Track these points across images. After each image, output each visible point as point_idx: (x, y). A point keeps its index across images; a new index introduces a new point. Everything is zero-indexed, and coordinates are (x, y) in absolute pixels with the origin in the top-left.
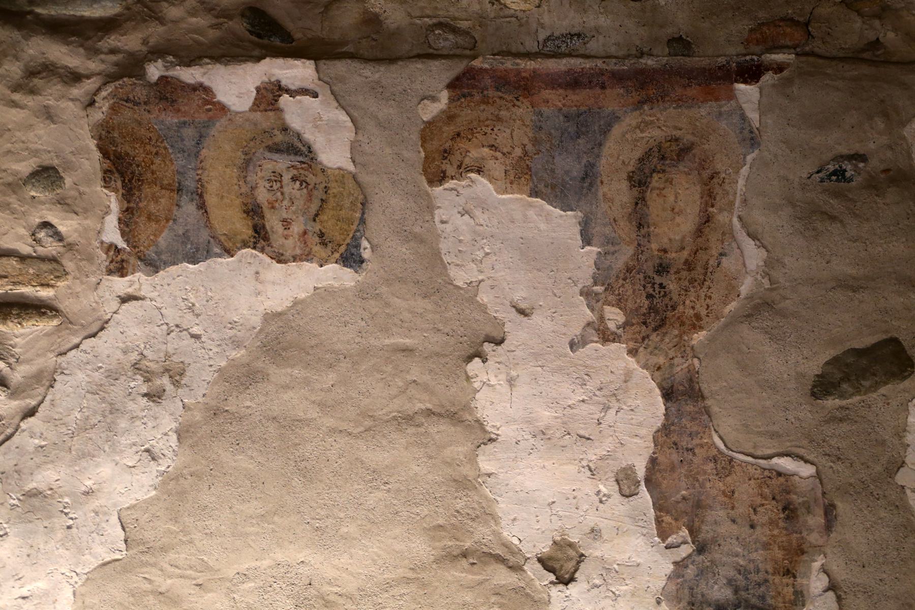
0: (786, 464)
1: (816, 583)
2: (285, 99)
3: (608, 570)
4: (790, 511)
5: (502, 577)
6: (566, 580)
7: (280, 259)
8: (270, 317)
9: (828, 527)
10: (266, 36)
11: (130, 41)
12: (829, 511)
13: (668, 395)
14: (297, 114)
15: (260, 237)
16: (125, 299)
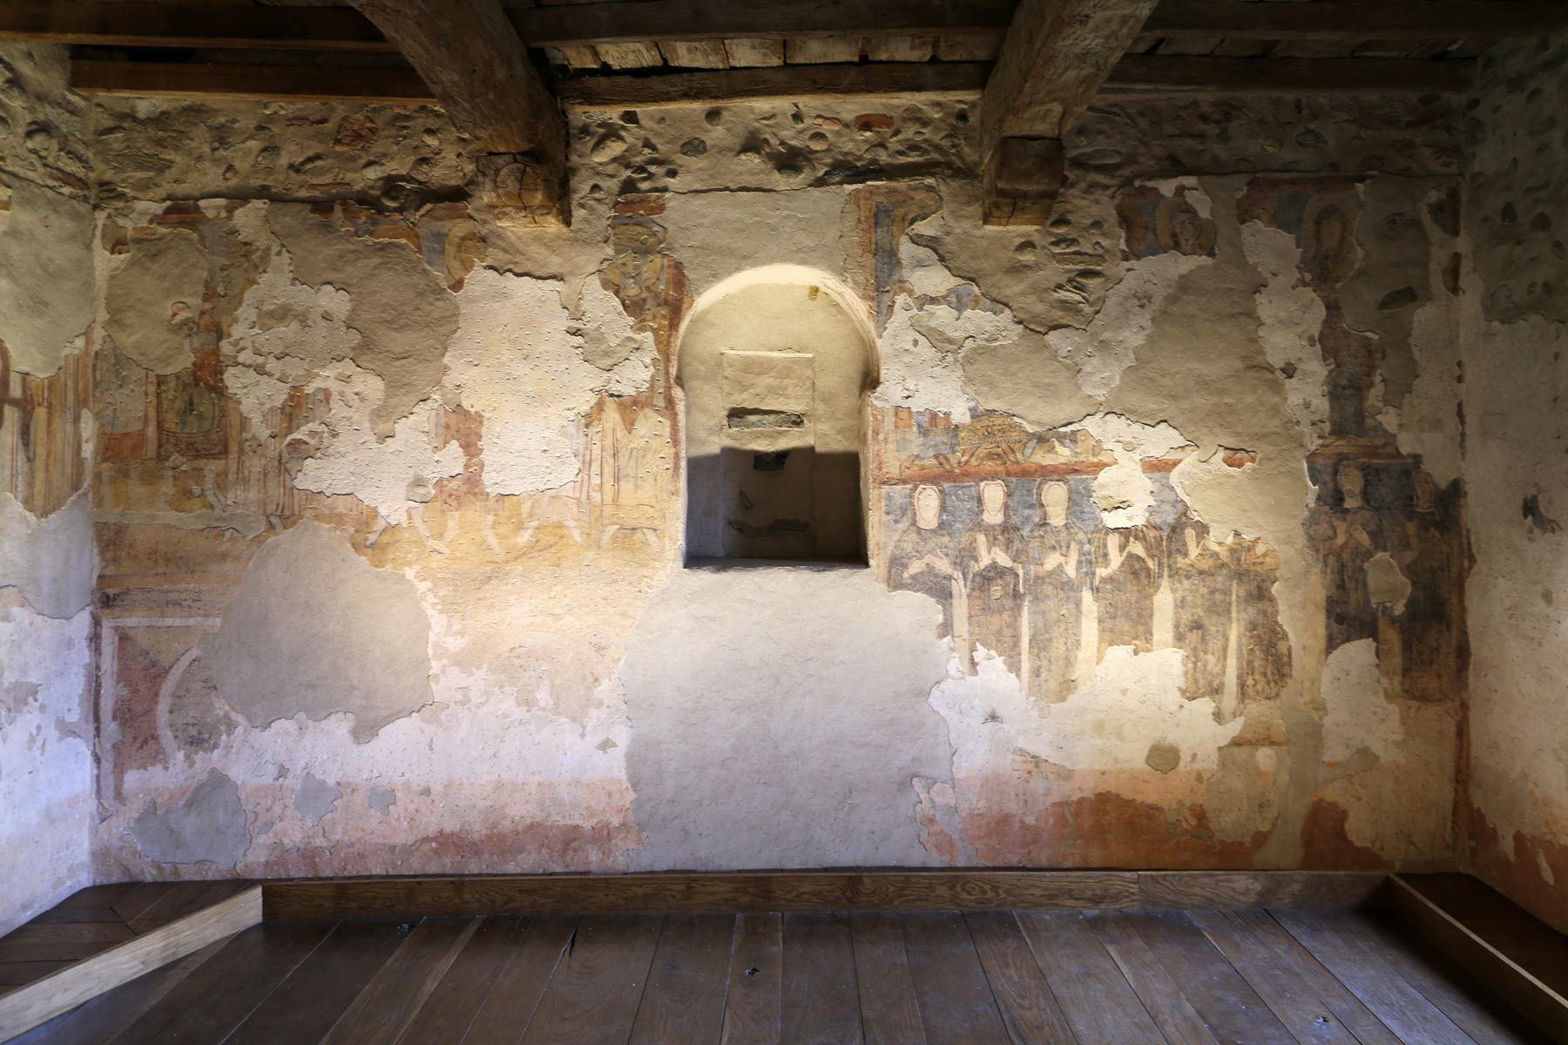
0: (1369, 334)
1: (1378, 379)
3: (1305, 373)
4: (1370, 353)
5: (1268, 375)
6: (1290, 377)
12: (1384, 352)
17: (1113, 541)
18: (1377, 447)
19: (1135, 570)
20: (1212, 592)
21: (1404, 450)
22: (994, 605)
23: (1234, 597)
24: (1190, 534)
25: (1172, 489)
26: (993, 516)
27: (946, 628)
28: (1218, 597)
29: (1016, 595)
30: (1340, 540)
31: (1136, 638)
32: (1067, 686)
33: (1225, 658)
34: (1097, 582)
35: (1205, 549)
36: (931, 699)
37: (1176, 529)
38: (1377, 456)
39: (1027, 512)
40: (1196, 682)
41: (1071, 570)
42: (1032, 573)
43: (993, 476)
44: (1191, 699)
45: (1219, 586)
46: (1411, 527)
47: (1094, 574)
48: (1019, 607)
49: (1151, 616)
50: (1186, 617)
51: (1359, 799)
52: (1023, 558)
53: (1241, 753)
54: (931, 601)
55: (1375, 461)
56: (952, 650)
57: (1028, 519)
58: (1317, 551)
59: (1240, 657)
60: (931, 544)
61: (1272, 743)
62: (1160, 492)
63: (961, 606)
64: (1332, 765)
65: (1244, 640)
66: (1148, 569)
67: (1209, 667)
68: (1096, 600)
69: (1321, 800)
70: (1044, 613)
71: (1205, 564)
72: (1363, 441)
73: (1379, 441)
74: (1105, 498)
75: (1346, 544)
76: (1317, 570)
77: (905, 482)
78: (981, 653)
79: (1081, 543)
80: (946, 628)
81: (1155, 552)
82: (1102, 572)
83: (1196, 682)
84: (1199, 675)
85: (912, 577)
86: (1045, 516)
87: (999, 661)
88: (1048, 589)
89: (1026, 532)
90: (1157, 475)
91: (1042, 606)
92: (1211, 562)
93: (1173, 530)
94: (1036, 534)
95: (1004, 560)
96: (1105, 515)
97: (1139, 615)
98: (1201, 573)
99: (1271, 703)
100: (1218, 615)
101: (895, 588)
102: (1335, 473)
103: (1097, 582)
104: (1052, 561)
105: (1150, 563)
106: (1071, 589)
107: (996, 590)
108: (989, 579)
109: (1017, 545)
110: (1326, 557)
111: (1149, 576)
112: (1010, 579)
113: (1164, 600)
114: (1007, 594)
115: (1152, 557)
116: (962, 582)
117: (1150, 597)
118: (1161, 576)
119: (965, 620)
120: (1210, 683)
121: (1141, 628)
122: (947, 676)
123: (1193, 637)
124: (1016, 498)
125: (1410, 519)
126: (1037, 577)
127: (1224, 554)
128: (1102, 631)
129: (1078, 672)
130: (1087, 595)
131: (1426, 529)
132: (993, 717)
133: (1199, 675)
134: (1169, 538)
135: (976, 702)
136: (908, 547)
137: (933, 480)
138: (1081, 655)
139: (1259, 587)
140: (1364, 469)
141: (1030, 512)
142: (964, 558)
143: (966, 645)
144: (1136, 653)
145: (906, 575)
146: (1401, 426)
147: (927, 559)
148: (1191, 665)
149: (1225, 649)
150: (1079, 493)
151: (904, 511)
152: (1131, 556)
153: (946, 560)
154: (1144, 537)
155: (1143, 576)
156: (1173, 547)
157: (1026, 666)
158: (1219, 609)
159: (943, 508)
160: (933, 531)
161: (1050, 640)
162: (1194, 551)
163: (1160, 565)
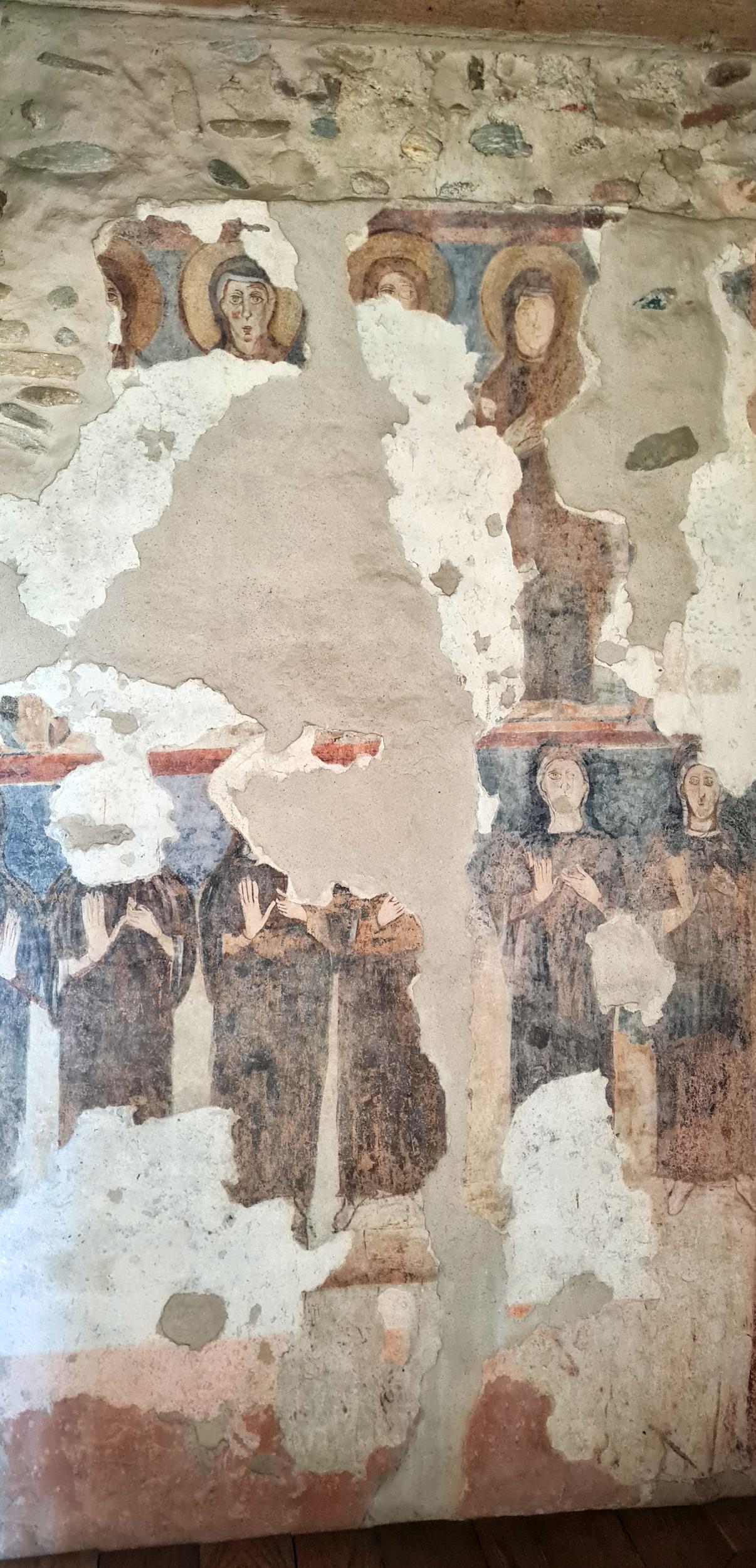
2: (244, 232)
5: (406, 591)
7: (242, 355)
8: (236, 400)
9: (631, 559)
10: (227, 179)
11: (127, 188)
13: (525, 463)
14: (254, 246)
15: (225, 341)
16: (127, 386)
18: (614, 722)
19: (134, 956)
20: (291, 998)
21: (666, 729)
23: (334, 1006)
24: (248, 889)
30: (543, 890)
34: (59, 986)
38: (614, 737)
46: (678, 866)
47: (53, 971)
51: (574, 1371)
53: (346, 1302)
55: (610, 748)
58: (496, 915)
59: (344, 1120)
61: (410, 1277)
64: (521, 1310)
65: (352, 1085)
66: (163, 958)
68: (56, 1021)
69: (503, 1379)
71: (275, 948)
72: (589, 711)
73: (619, 710)
75: (552, 898)
76: (494, 949)
82: (69, 967)
90: (181, 779)
99: (406, 1200)
102: (534, 770)
103: (59, 986)
105: (171, 948)
110: (512, 926)
113: (194, 1015)
115: (173, 934)
117: (164, 1010)
118: (189, 970)
123: (254, 1087)
125: (676, 850)
127: (316, 926)
130: (38, 1015)
131: (708, 869)
134: (207, 899)
139: (383, 985)
140: (588, 762)
144: (138, 1119)
146: (662, 682)
152: (128, 931)
154: (158, 899)
156: (214, 916)
162: (255, 919)
163: (189, 951)
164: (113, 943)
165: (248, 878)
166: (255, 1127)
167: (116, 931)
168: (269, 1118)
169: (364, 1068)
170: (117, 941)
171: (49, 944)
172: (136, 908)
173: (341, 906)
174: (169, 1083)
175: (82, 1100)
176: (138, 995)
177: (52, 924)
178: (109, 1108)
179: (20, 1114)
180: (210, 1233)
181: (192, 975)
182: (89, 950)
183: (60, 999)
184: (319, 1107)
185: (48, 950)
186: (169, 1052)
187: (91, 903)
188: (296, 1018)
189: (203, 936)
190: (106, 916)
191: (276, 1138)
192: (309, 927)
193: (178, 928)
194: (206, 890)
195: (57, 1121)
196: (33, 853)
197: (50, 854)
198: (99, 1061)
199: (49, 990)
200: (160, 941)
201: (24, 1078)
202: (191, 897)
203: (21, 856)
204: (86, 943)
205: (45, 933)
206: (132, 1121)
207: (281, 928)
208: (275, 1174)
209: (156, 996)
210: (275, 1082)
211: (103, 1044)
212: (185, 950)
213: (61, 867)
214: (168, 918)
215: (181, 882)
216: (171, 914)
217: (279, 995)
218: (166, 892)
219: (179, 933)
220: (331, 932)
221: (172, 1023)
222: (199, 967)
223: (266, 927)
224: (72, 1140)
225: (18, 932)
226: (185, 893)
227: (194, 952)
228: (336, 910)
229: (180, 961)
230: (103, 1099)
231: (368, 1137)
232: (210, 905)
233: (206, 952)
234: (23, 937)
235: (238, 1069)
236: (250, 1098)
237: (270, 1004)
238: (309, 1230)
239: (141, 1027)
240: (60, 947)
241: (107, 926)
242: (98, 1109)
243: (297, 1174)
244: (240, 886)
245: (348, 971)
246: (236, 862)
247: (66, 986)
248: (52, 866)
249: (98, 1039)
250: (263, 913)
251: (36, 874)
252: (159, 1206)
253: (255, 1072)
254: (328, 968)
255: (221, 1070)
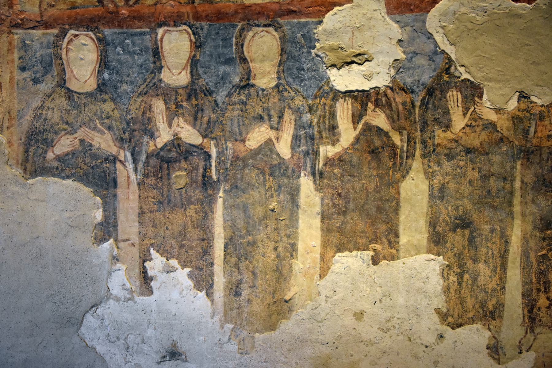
17: (344, 111)
19: (373, 145)
20: (485, 177)
22: (176, 197)
23: (518, 184)
24: (454, 97)
25: (430, 36)
26: (176, 75)
27: (107, 229)
28: (493, 183)
29: (207, 183)
31: (375, 240)
32: (280, 308)
33: (504, 267)
34: (320, 164)
35: (476, 117)
36: (83, 330)
37: (435, 92)
39: (222, 69)
40: (462, 301)
41: (284, 148)
42: (230, 152)
43: (175, 20)
44: (454, 326)
45: (495, 169)
47: (316, 153)
48: (211, 200)
49: (397, 209)
50: (446, 212)
52: (217, 132)
54: (86, 190)
56: (116, 259)
57: (224, 78)
59: (525, 267)
60: (87, 113)
62: (412, 40)
63: (129, 199)
65: (532, 244)
66: (393, 146)
67: (481, 280)
68: (319, 189)
70: (245, 208)
71: (475, 140)
74: (333, 49)
77: (47, 26)
78: (156, 263)
79: (298, 112)
80: (107, 229)
81: (403, 123)
82: (328, 151)
83: (462, 301)
84: (465, 292)
85: (59, 158)
86: (248, 74)
87: (182, 275)
88: (252, 175)
89: (221, 97)
90: (408, 17)
91: (244, 198)
92: (484, 136)
93: (430, 92)
94: (235, 99)
95: (190, 135)
96: (333, 73)
97: (379, 209)
98: (469, 151)
100: (495, 208)
101: (34, 174)
103: (320, 164)
104: (257, 136)
105: (396, 139)
106: (284, 174)
107: (179, 177)
108: (169, 161)
109: (208, 114)
111: (394, 155)
112: (198, 161)
113: (414, 188)
114: (193, 181)
115: (400, 130)
116: (130, 166)
117: (395, 184)
118: (411, 155)
119: (134, 217)
120: (483, 304)
121: (383, 227)
122: (108, 295)
123: (457, 239)
124: (207, 50)
126: (236, 158)
127: (504, 124)
128: (327, 231)
129: (295, 289)
130: (306, 184)
132: (174, 354)
133: (465, 292)
134: (424, 104)
135: (150, 332)
136: (54, 116)
137: (89, 23)
138: (298, 265)
141: (227, 69)
142: (135, 131)
143: (135, 252)
144: (375, 261)
145: (50, 155)
147: (80, 134)
148: (453, 278)
149: (504, 255)
150: (294, 42)
151: (47, 67)
152: (368, 128)
153: (108, 135)
154: (389, 104)
155: (385, 156)
156: (429, 116)
157: (220, 280)
158: (496, 201)
159: (104, 63)
160: (89, 95)
161: (254, 244)
162: (459, 122)
164: (357, 136)
165: (454, 89)
166: (459, 270)
167: (360, 126)
168: (470, 264)
169: (541, 231)
170: (360, 134)
171: (313, 135)
172: (374, 111)
173: (523, 110)
174: (397, 236)
175: (336, 246)
176: (375, 173)
177: (316, 120)
178: (355, 253)
179: (294, 254)
180: (427, 347)
181: (413, 159)
182: (341, 139)
183: (321, 174)
184: (506, 258)
185: (313, 138)
186: (397, 214)
187: (342, 106)
188: (489, 192)
189: (421, 131)
190: (353, 116)
191: (475, 279)
192: (498, 126)
193: (403, 126)
194: (424, 98)
195: (318, 260)
196: (303, 69)
197: (315, 70)
198: (348, 218)
199: (313, 167)
200: (390, 134)
201: (297, 228)
202: (413, 103)
203: (295, 71)
204: (339, 134)
205: (310, 126)
206: (371, 262)
207: (478, 126)
208: (474, 306)
209: (387, 174)
210: (474, 238)
211: (351, 206)
212: (409, 141)
213: (322, 80)
214: (395, 117)
215: (406, 92)
216: (398, 116)
217: (476, 175)
218: (394, 99)
219: (404, 129)
220: (515, 131)
221: (399, 193)
222: (418, 153)
223: (467, 125)
224: (328, 275)
225: (293, 126)
226: (408, 100)
227: (415, 143)
228: (520, 114)
229: (405, 149)
230: (351, 246)
231: (545, 282)
232: (427, 108)
233: (424, 142)
234: (295, 129)
235: (447, 228)
236: (456, 249)
237: (470, 182)
238: (500, 350)
239: (377, 195)
240: (321, 137)
241: (354, 123)
242: (347, 253)
243: (491, 308)
244: (448, 95)
245: (528, 159)
246: (446, 77)
247: (325, 165)
248: (315, 78)
249: (348, 202)
250: (465, 115)
251: (305, 85)
252: (390, 324)
253: (459, 230)
254: (513, 156)
255: (435, 228)
